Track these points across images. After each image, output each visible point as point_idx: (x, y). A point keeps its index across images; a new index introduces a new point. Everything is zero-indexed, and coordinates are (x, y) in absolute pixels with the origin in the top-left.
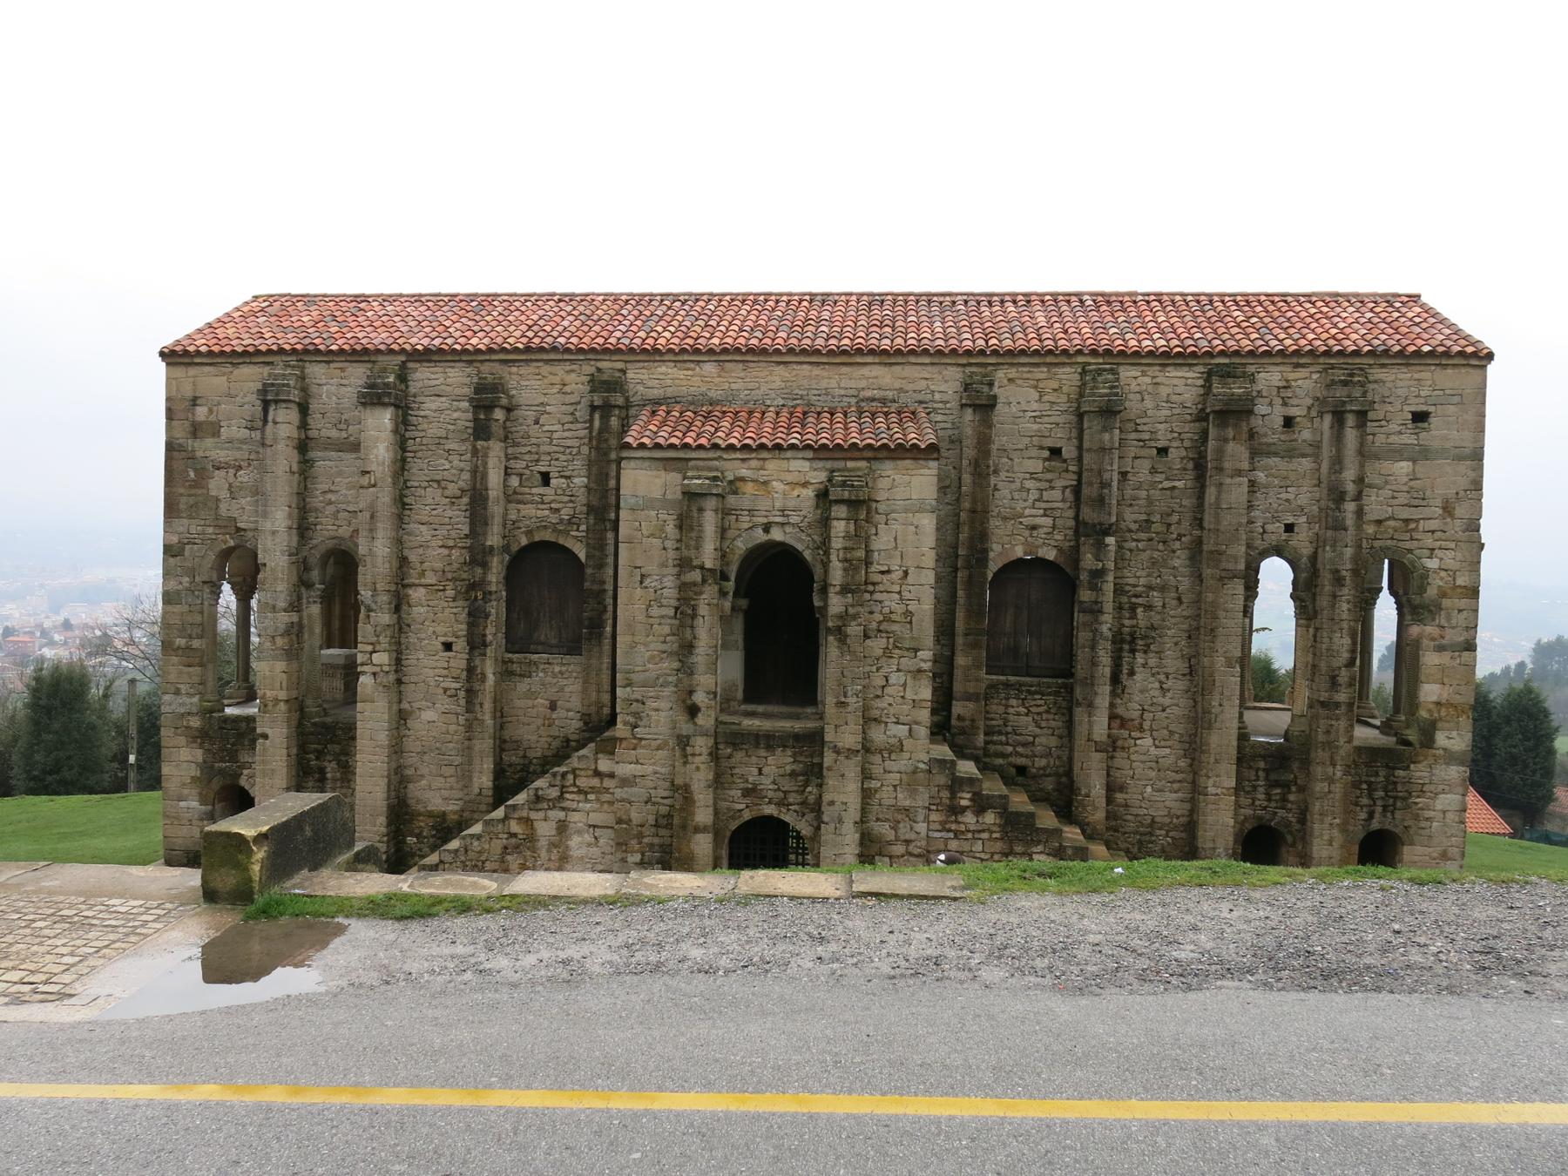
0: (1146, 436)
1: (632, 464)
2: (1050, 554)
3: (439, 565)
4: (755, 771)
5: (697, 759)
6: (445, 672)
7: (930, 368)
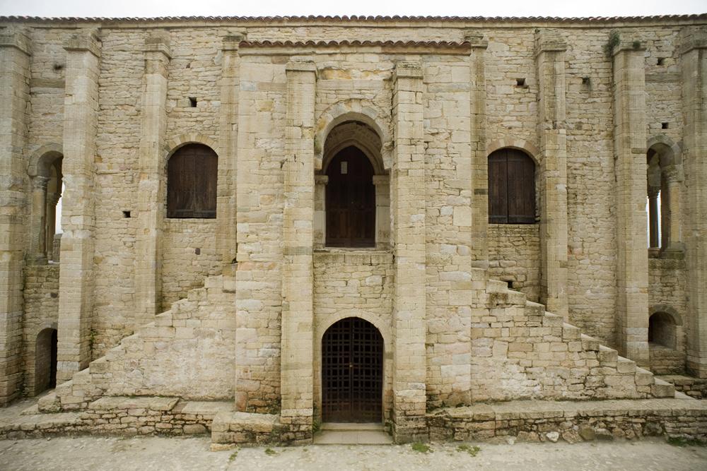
0: (574, 71)
1: (250, 59)
2: (520, 144)
3: (121, 160)
4: (343, 284)
6: (125, 231)
7: (441, 31)
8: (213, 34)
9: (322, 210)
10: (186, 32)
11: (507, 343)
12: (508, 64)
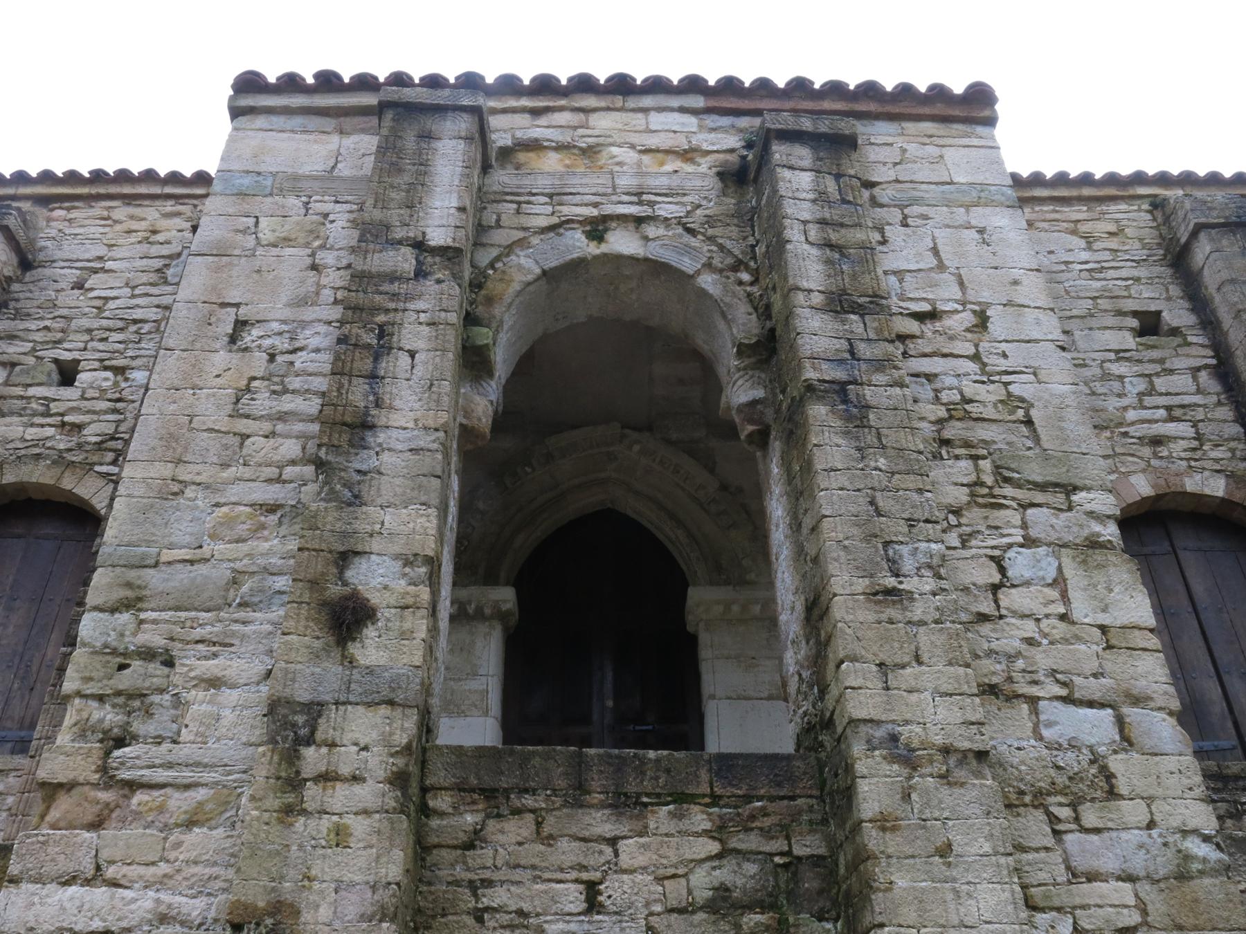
4: (573, 898)
5: (340, 797)
8: (178, 214)
9: (486, 713)
10: (99, 209)
12: (1093, 279)
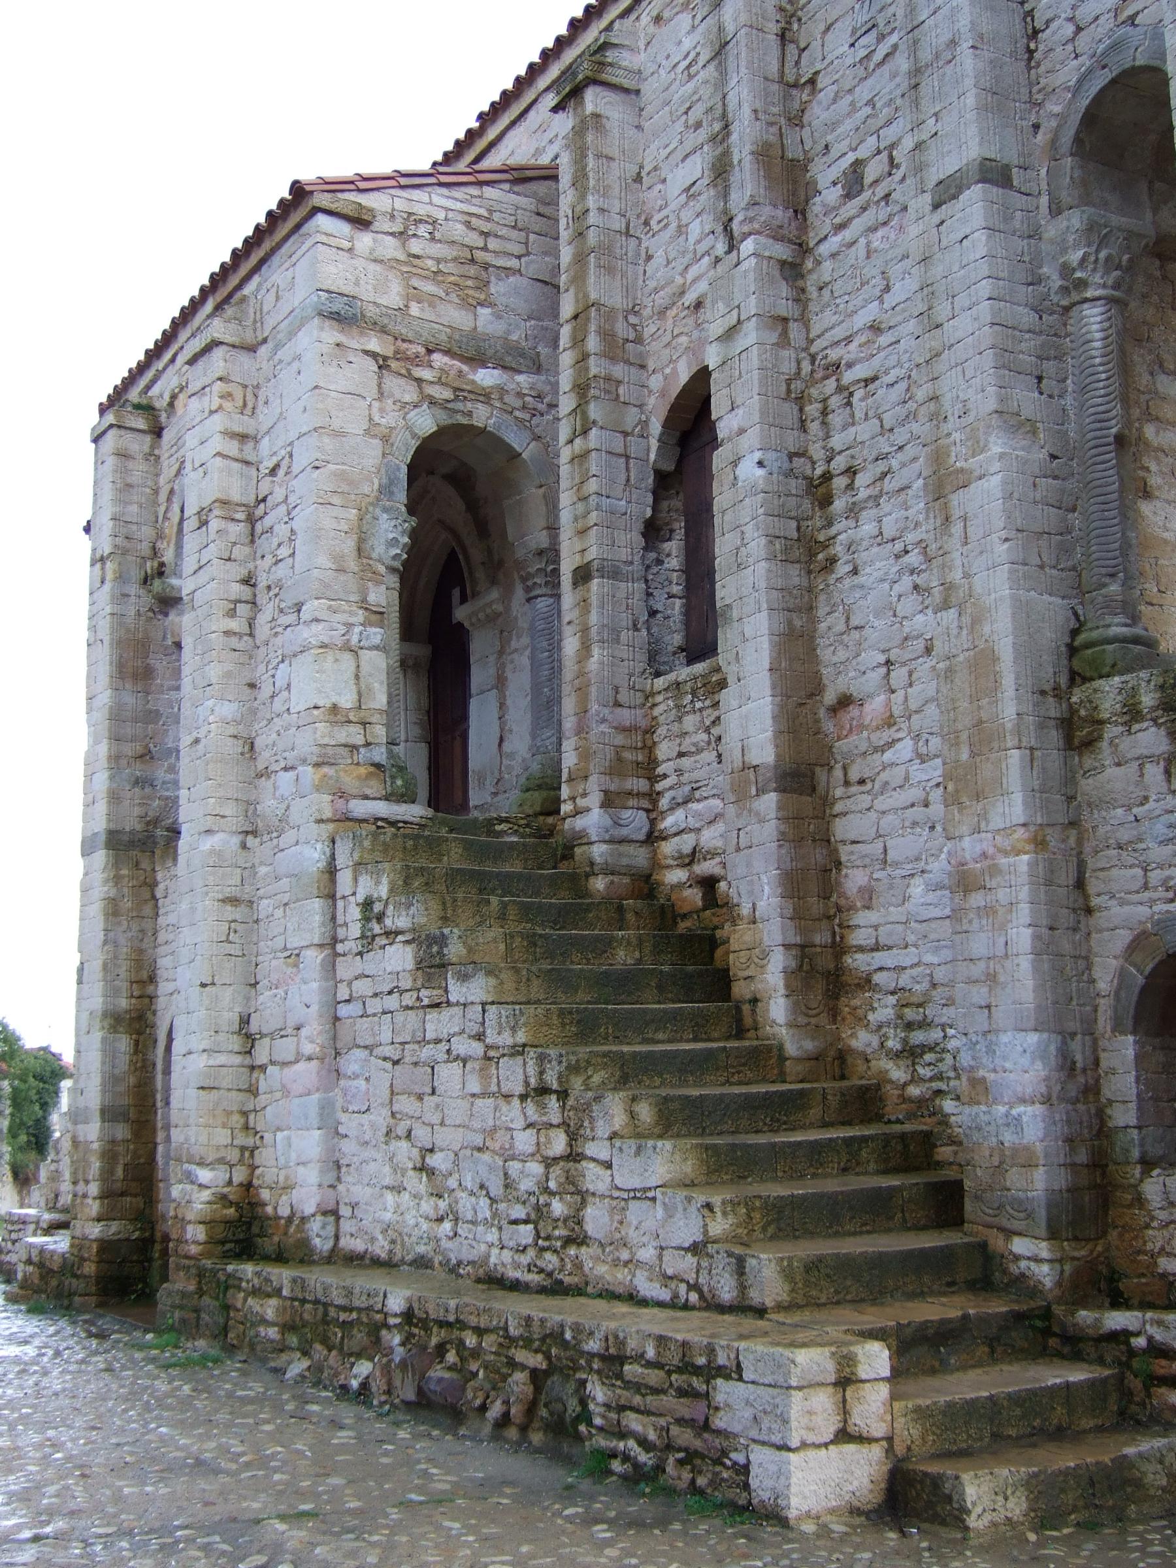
11: (389, 1065)
